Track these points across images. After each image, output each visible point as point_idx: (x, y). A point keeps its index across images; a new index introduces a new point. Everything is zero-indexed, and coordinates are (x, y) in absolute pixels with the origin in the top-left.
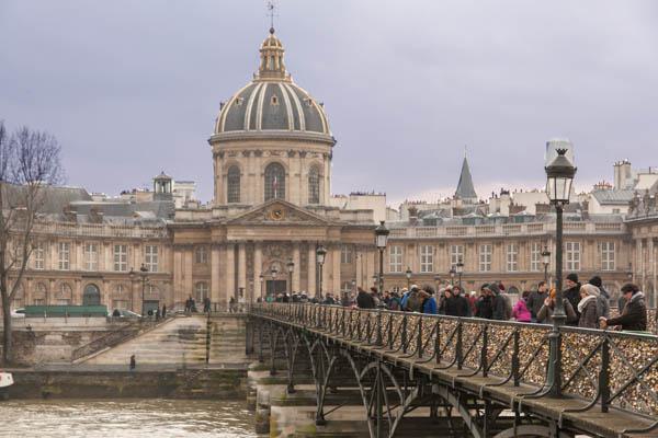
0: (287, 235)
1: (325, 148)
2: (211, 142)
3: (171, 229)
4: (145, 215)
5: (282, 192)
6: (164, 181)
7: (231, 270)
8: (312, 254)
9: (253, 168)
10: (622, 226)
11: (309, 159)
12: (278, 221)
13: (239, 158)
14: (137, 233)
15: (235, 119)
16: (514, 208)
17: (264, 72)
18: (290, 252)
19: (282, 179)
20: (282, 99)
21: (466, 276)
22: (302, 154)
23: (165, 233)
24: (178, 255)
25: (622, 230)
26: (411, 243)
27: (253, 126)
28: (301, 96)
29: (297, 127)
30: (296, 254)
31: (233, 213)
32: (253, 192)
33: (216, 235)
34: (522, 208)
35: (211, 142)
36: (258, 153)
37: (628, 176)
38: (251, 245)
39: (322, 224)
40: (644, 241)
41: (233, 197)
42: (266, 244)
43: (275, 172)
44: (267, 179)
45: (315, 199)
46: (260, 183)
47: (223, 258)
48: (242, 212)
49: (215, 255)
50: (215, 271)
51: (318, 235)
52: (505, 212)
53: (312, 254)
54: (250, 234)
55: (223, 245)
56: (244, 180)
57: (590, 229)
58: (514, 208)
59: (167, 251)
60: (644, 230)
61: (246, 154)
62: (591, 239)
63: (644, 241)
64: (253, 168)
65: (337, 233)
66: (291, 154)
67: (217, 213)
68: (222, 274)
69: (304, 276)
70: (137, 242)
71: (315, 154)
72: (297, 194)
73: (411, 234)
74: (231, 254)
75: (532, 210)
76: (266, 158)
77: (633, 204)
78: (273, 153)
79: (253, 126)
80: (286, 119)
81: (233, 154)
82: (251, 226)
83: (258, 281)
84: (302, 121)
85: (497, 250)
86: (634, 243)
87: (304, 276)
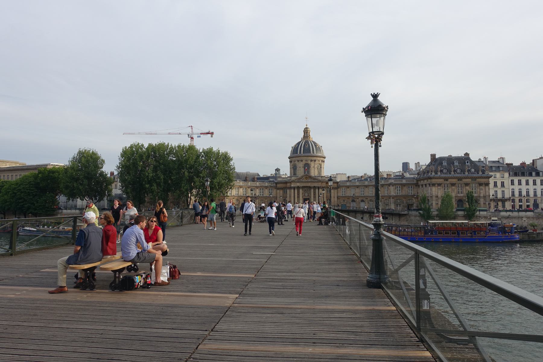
0: (309, 185)
1: (322, 159)
2: (289, 158)
3: (276, 183)
4: (271, 180)
5: (309, 172)
6: (278, 170)
7: (293, 195)
8: (317, 190)
9: (300, 165)
10: (415, 181)
11: (317, 162)
12: (306, 181)
13: (296, 162)
14: (267, 184)
15: (295, 150)
17: (304, 137)
18: (310, 190)
19: (309, 168)
20: (309, 145)
21: (365, 197)
22: (315, 161)
23: (275, 185)
24: (278, 191)
25: (415, 182)
26: (348, 187)
27: (300, 153)
28: (315, 143)
29: (313, 153)
30: (312, 190)
31: (293, 178)
32: (301, 172)
33: (288, 184)
35: (289, 158)
36: (302, 161)
37: (419, 166)
38: (298, 188)
39: (320, 181)
40: (422, 185)
41: (295, 174)
42: (303, 187)
43: (307, 167)
44: (305, 168)
45: (320, 173)
46: (302, 169)
47: (290, 192)
48: (296, 178)
49: (288, 191)
50: (288, 196)
51: (319, 185)
53: (317, 190)
54: (298, 184)
55: (290, 188)
56: (298, 168)
57: (404, 181)
59: (275, 190)
60: (422, 182)
61: (298, 161)
63: (422, 185)
64: (300, 165)
65: (325, 184)
66: (311, 161)
67: (289, 178)
68: (290, 197)
69: (315, 197)
70: (266, 187)
71: (319, 161)
72: (314, 173)
73: (348, 184)
74: (292, 191)
75: (386, 176)
76: (304, 162)
77: (418, 174)
78: (306, 161)
79: (300, 153)
80: (310, 150)
81: (295, 161)
82: (298, 182)
83: (301, 198)
84: (315, 151)
86: (419, 186)
87: (315, 197)
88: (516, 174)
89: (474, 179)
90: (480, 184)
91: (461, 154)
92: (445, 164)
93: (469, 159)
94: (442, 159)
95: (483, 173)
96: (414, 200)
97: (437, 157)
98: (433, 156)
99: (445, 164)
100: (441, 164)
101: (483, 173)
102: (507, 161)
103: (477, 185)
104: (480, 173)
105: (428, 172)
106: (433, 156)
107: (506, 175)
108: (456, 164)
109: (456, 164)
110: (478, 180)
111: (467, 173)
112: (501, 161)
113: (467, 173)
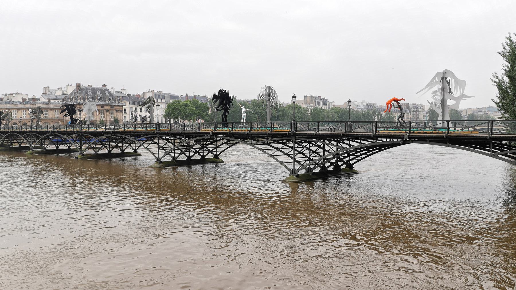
16: (24, 99)
34: (26, 99)
37: (49, 91)
52: (21, 101)
57: (51, 106)
58: (24, 99)
62: (52, 109)
85: (19, 112)
88: (134, 103)
89: (112, 106)
90: (117, 111)
91: (100, 86)
92: (90, 93)
93: (107, 90)
94: (87, 89)
95: (119, 102)
96: (61, 123)
97: (81, 86)
98: (78, 85)
99: (90, 93)
100: (87, 93)
101: (119, 102)
102: (128, 92)
103: (114, 111)
104: (117, 102)
105: (76, 99)
106: (78, 85)
107: (128, 103)
108: (99, 94)
109: (99, 94)
110: (115, 107)
111: (107, 102)
112: (123, 92)
113: (107, 102)
